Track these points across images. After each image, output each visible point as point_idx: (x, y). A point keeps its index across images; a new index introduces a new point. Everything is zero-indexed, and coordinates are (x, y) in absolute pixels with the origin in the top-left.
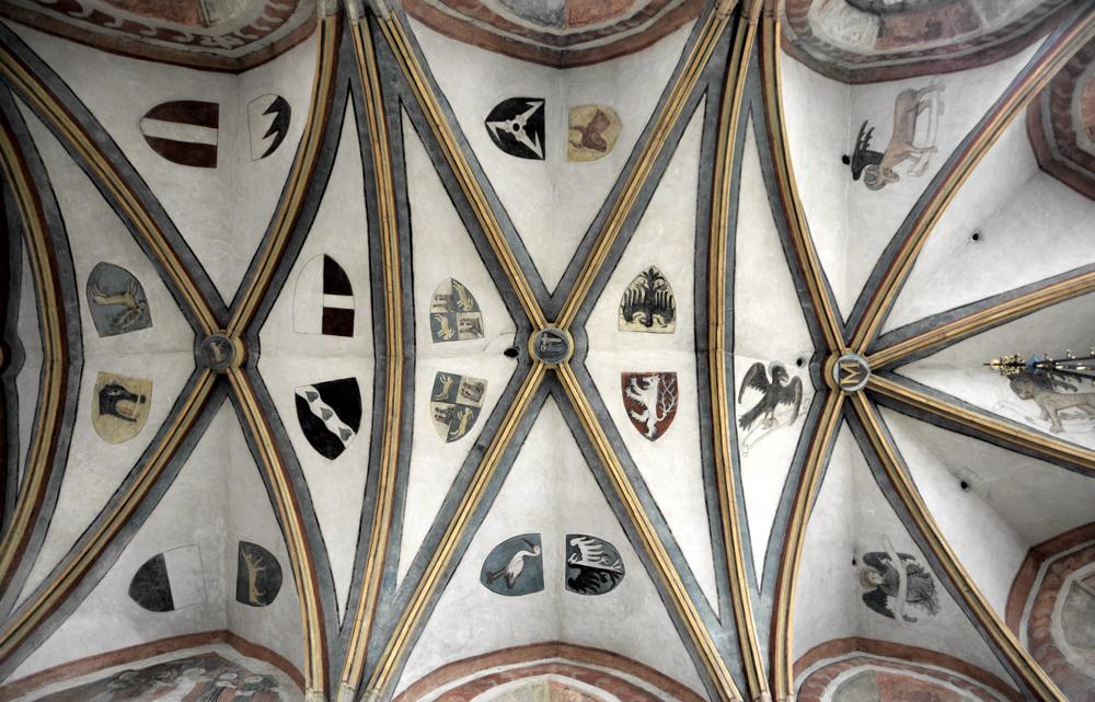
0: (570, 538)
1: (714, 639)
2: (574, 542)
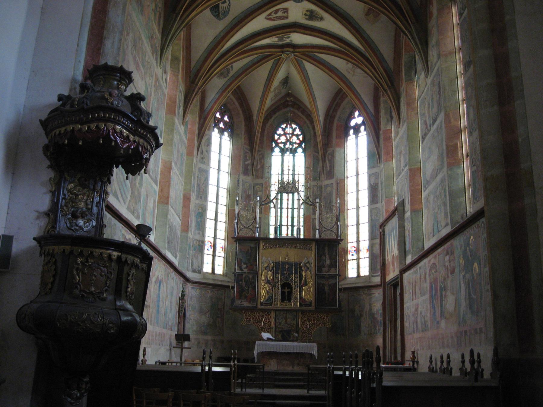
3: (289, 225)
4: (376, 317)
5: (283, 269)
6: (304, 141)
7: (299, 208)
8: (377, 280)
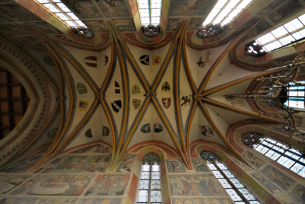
0: (154, 124)
1: (177, 140)
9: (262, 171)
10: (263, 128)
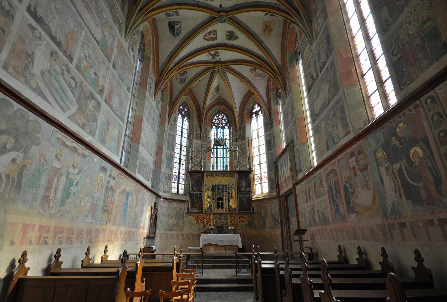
2: (179, 23)
3: (219, 158)
4: (275, 217)
5: (218, 189)
6: (228, 122)
7: (227, 154)
8: (275, 194)
9: (169, 133)
10: (195, 119)
